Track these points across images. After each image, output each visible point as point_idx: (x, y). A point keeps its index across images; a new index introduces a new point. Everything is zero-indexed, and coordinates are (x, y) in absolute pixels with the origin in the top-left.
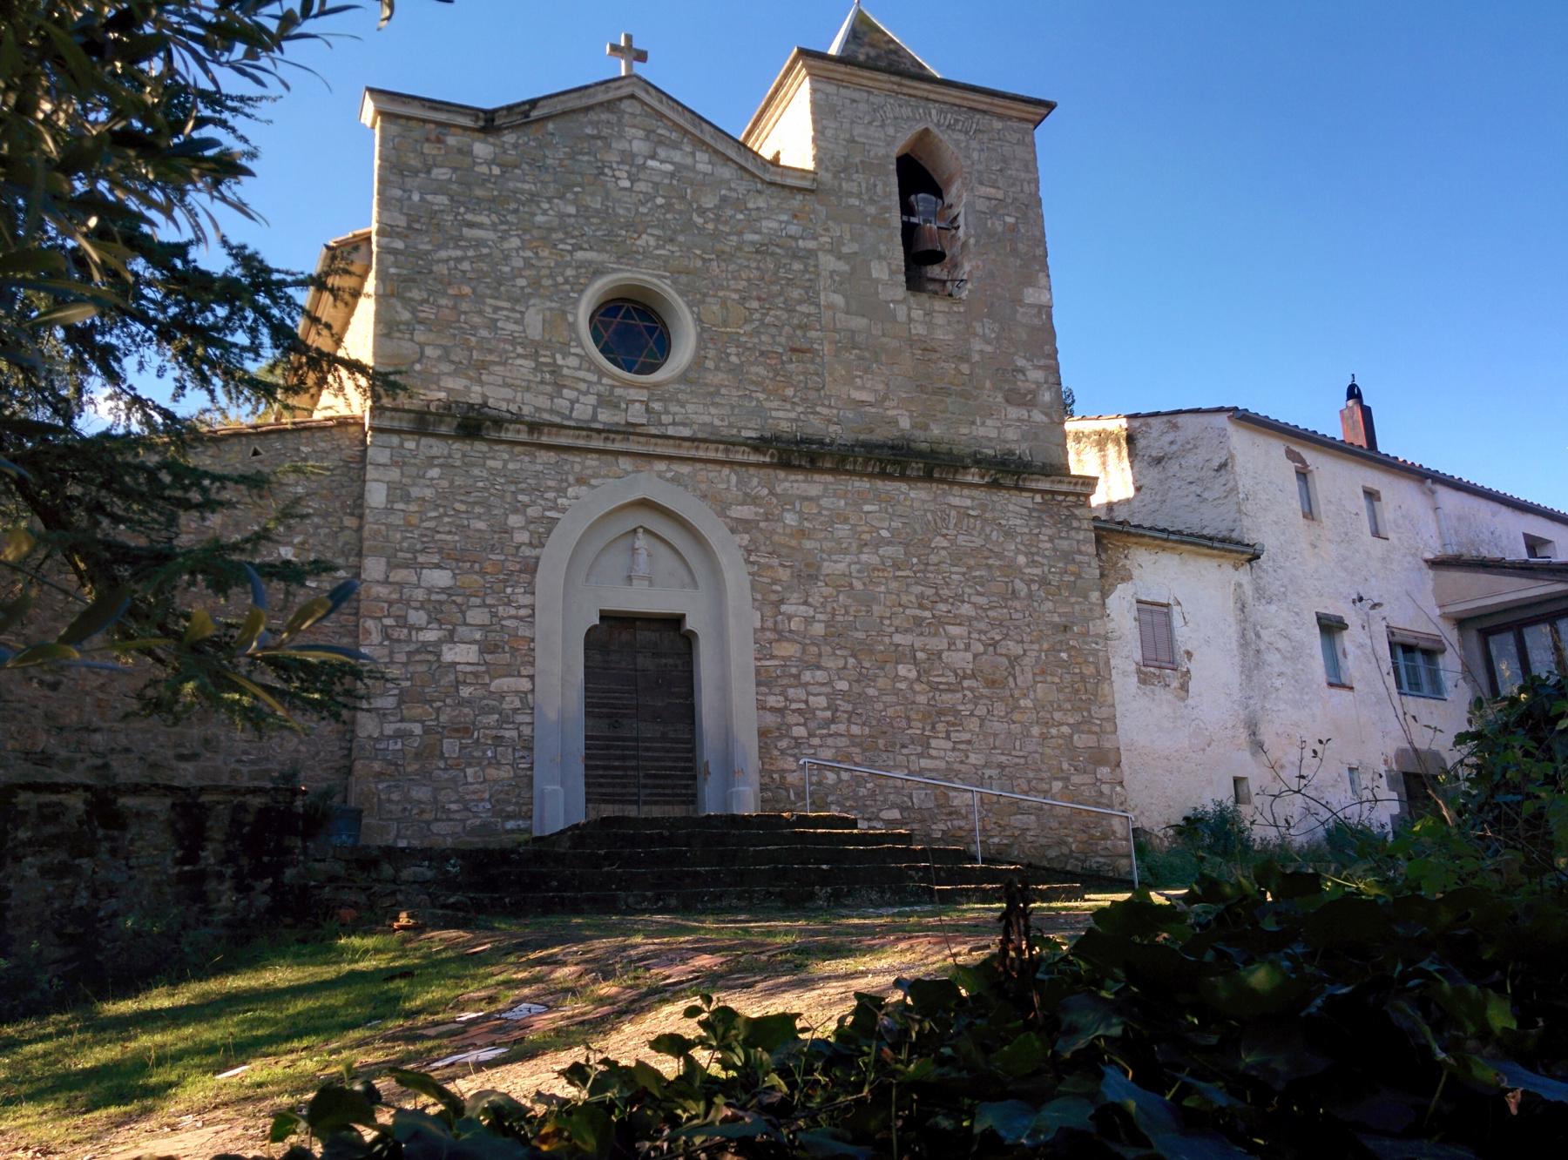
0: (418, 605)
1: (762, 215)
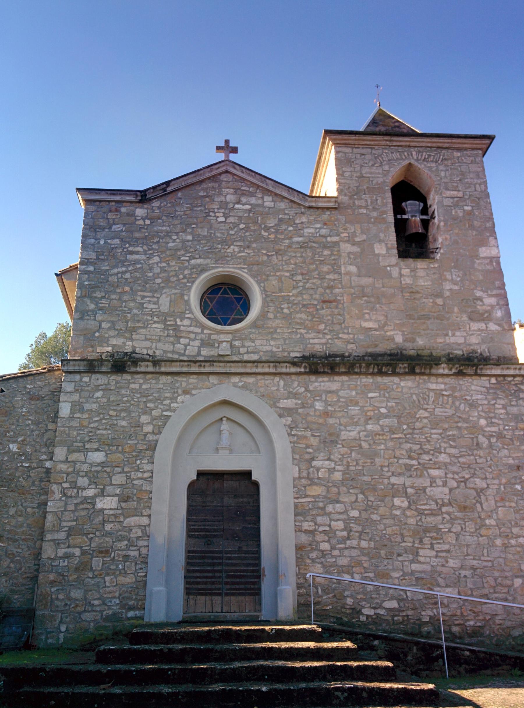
0: (84, 474)
1: (305, 226)
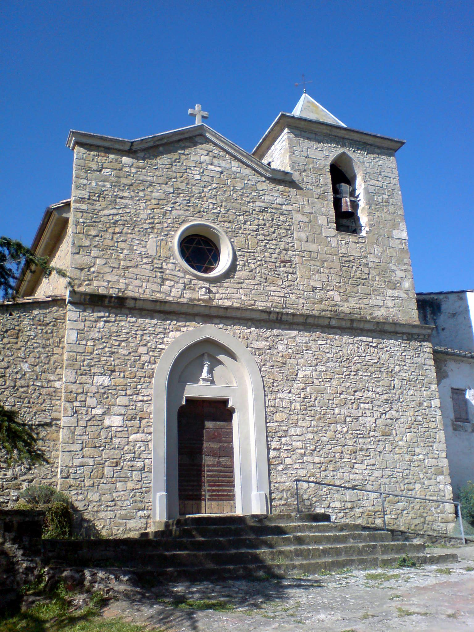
0: (92, 395)
